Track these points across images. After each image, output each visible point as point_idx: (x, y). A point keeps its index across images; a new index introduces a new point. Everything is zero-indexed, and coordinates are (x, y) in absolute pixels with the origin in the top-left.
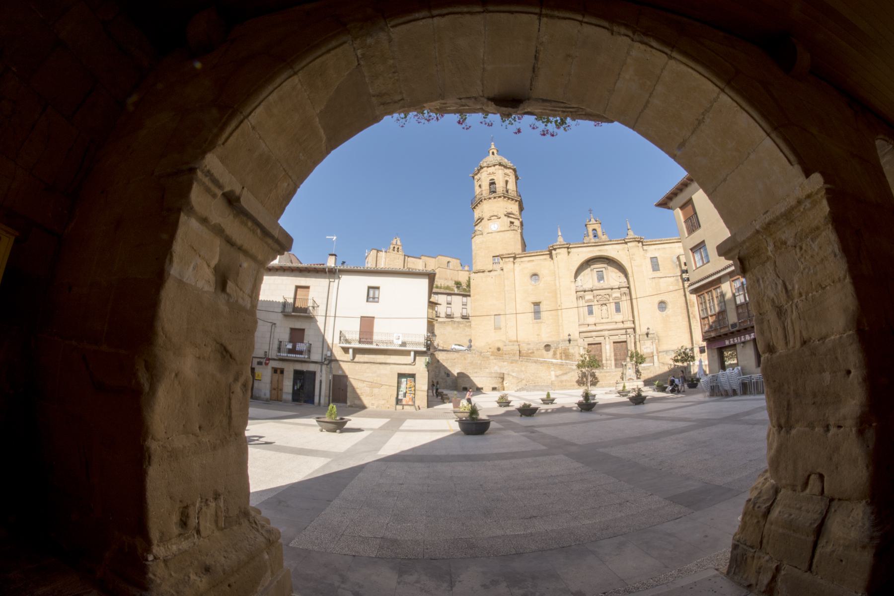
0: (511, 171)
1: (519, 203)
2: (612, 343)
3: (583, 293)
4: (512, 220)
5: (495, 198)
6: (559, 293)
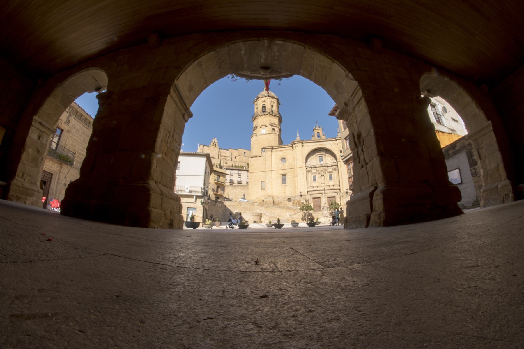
0: (275, 99)
1: (279, 118)
3: (310, 169)
4: (274, 128)
5: (264, 115)
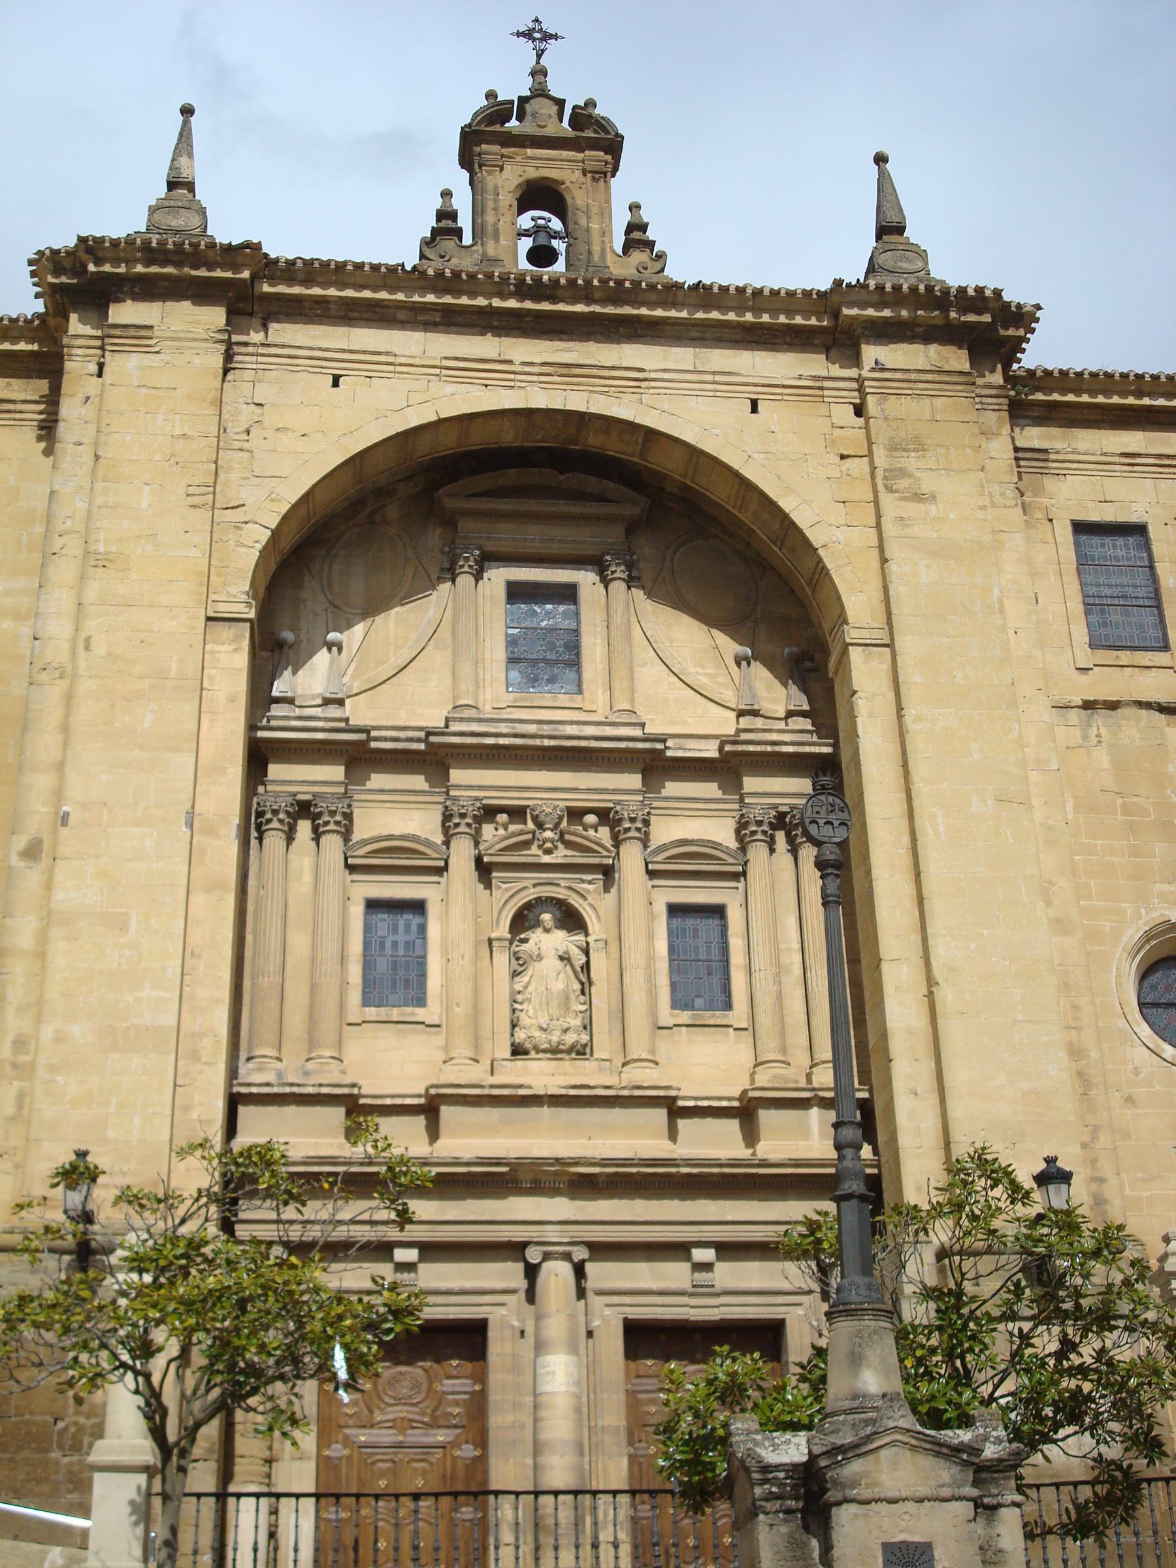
2: (613, 1342)
6: (53, 716)
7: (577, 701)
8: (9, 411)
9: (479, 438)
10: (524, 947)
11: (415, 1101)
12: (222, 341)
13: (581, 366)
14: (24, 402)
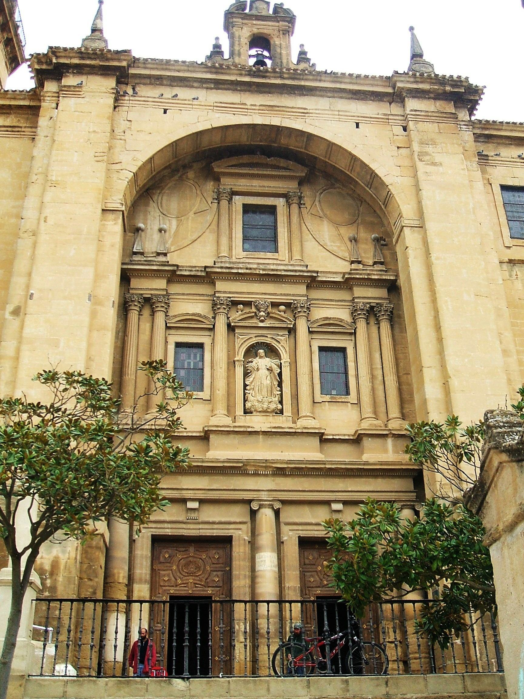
3: (161, 284)
7: (276, 255)
8: (18, 131)
9: (231, 139)
10: (250, 364)
11: (198, 435)
12: (113, 93)
13: (278, 107)
14: (25, 127)
